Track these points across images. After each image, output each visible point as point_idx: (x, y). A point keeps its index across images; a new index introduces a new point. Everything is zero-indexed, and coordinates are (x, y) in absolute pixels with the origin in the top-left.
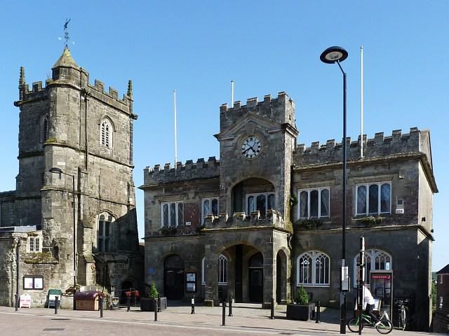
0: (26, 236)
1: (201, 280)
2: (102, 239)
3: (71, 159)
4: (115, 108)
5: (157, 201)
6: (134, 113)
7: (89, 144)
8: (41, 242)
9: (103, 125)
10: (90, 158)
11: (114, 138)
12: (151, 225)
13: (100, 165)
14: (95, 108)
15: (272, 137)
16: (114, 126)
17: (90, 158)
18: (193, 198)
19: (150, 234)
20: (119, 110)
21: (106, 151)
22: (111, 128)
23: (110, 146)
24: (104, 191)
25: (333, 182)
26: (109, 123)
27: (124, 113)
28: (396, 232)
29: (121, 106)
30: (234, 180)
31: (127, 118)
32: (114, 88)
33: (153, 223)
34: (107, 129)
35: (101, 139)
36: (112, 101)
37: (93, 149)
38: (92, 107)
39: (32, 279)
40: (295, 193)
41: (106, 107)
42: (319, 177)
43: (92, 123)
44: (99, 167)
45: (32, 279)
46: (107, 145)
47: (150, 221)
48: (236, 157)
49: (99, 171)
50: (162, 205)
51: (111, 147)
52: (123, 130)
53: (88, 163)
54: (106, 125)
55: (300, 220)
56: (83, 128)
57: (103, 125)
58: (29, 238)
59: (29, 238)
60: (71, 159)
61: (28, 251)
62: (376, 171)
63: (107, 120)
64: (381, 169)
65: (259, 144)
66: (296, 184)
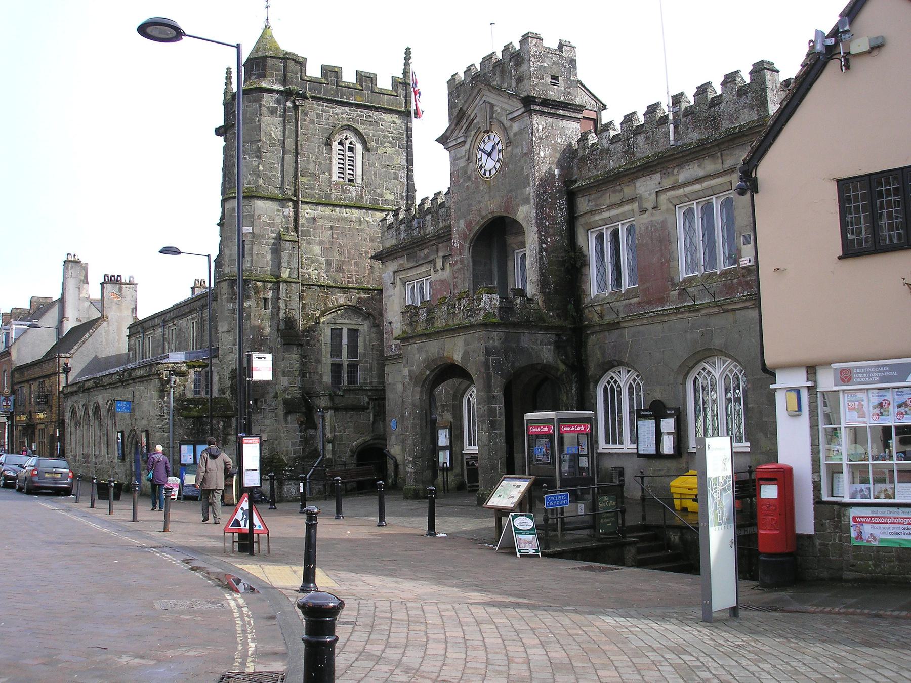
1: (462, 442)
3: (264, 218)
5: (398, 282)
8: (215, 378)
9: (341, 143)
10: (307, 212)
11: (366, 168)
13: (330, 219)
14: (319, 116)
15: (516, 127)
17: (307, 212)
18: (443, 269)
20: (377, 109)
21: (344, 191)
22: (359, 147)
23: (359, 180)
24: (339, 269)
25: (635, 206)
26: (353, 138)
27: (391, 111)
28: (743, 312)
29: (384, 102)
30: (469, 225)
32: (367, 69)
34: (351, 149)
38: (312, 115)
39: (191, 447)
40: (581, 241)
41: (347, 109)
42: (616, 198)
43: (311, 147)
44: (329, 224)
45: (191, 447)
48: (469, 178)
49: (330, 232)
50: (408, 288)
51: (359, 180)
53: (301, 221)
55: (596, 297)
56: (289, 158)
58: (192, 371)
60: (264, 218)
62: (701, 173)
63: (349, 134)
64: (710, 166)
65: (500, 147)
66: (582, 221)
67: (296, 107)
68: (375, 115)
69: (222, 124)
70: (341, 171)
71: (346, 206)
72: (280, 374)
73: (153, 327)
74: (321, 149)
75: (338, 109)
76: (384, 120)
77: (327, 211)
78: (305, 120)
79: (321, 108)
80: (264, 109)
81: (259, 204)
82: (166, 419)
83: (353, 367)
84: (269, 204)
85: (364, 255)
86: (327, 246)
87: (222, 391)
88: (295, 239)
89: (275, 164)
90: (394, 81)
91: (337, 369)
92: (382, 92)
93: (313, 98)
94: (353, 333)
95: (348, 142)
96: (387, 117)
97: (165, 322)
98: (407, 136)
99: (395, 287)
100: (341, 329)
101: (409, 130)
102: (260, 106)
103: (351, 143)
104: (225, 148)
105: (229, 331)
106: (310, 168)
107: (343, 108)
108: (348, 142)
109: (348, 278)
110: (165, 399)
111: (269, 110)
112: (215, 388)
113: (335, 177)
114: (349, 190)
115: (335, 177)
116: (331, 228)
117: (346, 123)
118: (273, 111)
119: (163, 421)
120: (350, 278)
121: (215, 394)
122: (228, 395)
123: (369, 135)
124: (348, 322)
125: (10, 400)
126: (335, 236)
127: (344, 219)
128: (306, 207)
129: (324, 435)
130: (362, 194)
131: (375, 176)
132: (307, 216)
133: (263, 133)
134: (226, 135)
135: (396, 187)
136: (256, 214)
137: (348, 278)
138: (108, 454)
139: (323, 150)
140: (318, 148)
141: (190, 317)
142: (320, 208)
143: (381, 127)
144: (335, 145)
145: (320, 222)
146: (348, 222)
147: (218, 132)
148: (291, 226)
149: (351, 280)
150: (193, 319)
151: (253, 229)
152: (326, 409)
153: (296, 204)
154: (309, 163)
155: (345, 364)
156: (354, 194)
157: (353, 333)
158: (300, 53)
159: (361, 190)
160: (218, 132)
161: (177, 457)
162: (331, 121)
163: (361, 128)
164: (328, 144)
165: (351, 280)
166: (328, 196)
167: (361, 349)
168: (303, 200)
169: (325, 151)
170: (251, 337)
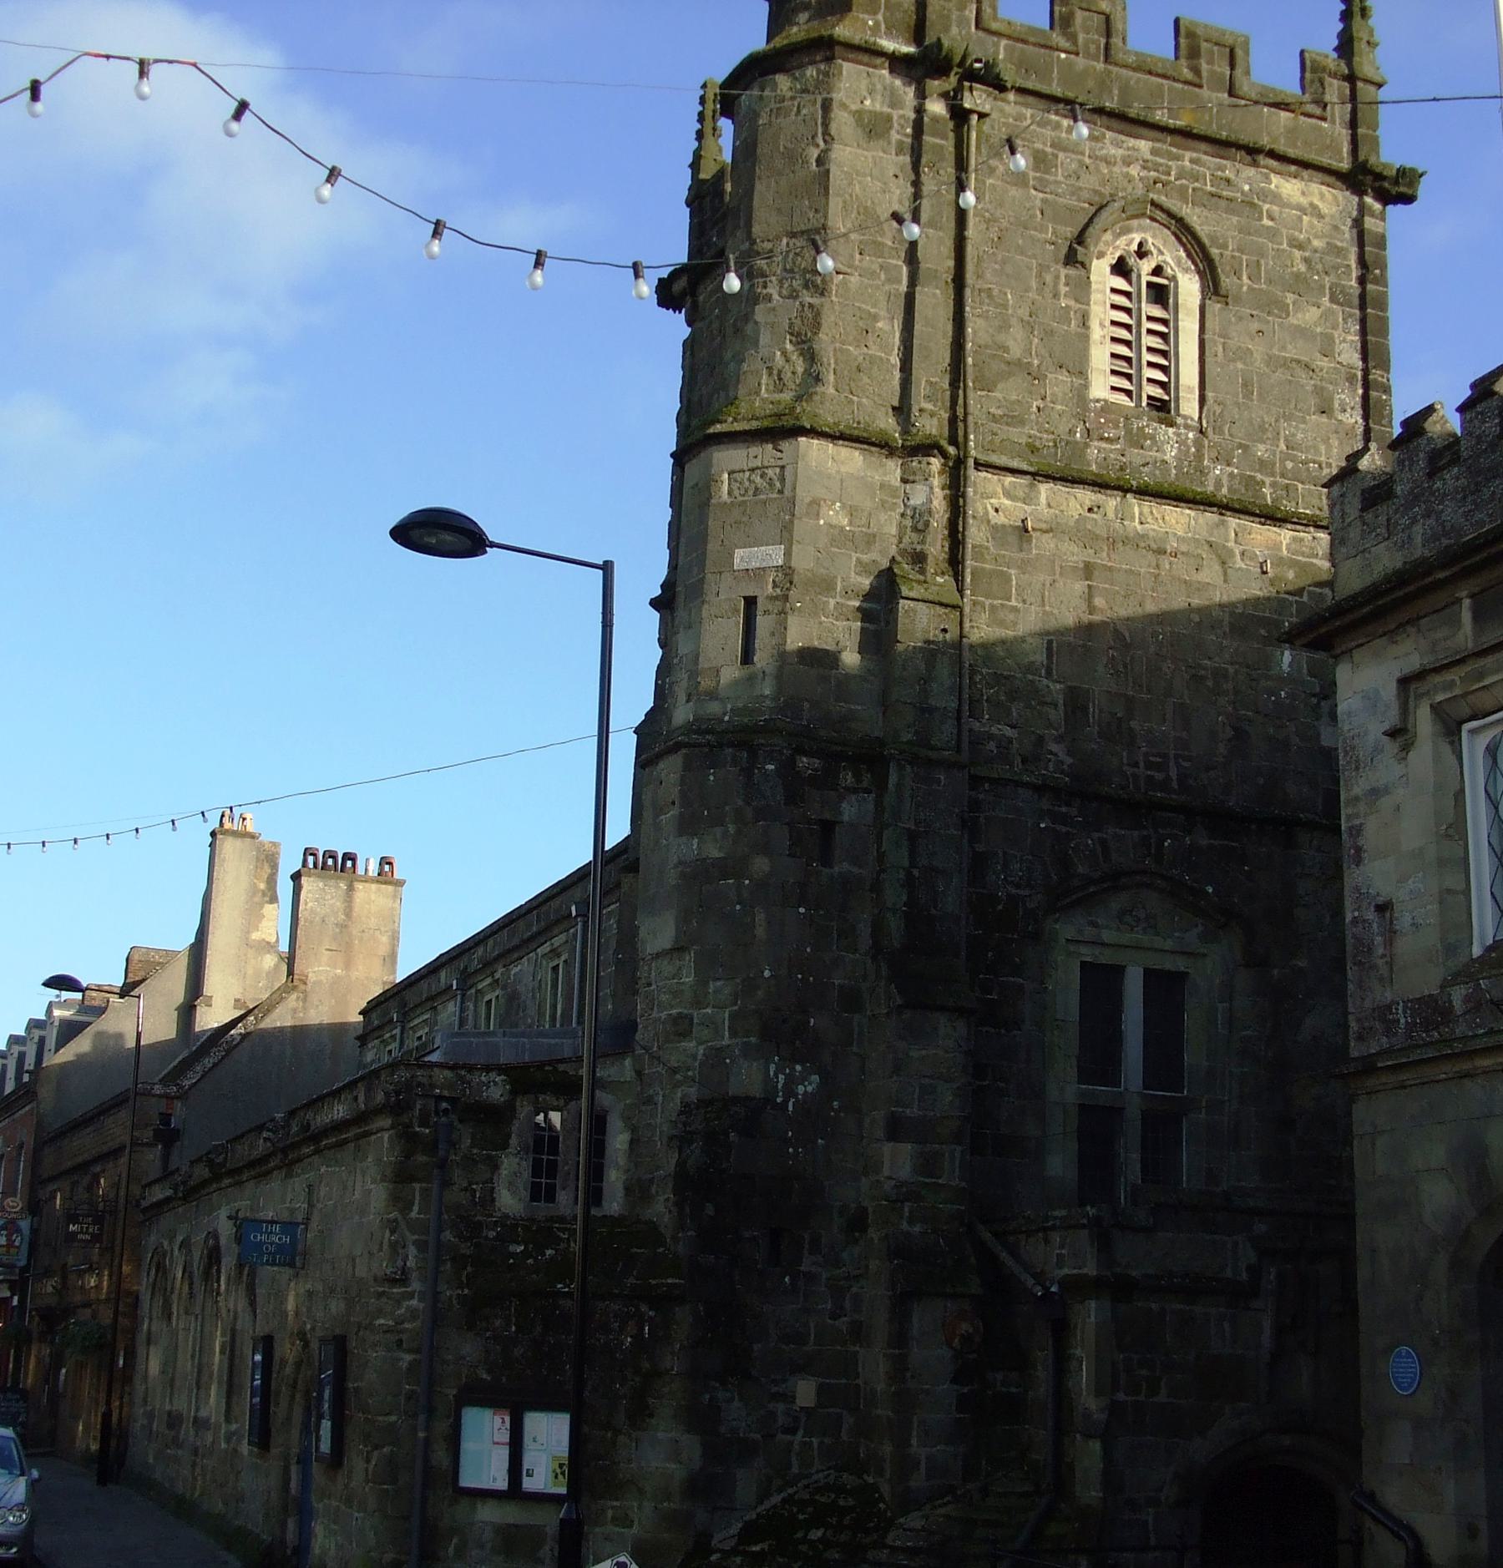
0: (496, 1090)
4: (1222, 145)
5: (1424, 722)
6: (1390, 154)
7: (977, 402)
8: (618, 1141)
9: (1121, 268)
11: (1216, 348)
12: (1391, 934)
13: (1083, 535)
14: (1040, 161)
19: (1390, 1026)
20: (1252, 152)
21: (1137, 440)
22: (1189, 288)
23: (1189, 406)
26: (1169, 254)
29: (1276, 128)
31: (1332, 201)
33: (1404, 921)
34: (1160, 294)
35: (1100, 356)
37: (1019, 435)
41: (1144, 146)
47: (1383, 908)
49: (1080, 586)
52: (1299, 285)
53: (975, 534)
56: (934, 302)
60: (835, 515)
61: (509, 1201)
67: (960, 116)
68: (1245, 177)
70: (1125, 366)
71: (1143, 492)
73: (432, 998)
74: (1049, 278)
75: (1115, 145)
76: (1276, 198)
78: (992, 170)
79: (1048, 133)
80: (842, 121)
81: (812, 449)
82: (411, 1296)
84: (851, 459)
85: (1210, 683)
87: (637, 1191)
88: (954, 598)
89: (875, 318)
93: (1022, 91)
95: (1146, 266)
96: (1290, 188)
97: (466, 979)
98: (1362, 262)
99: (1406, 748)
100: (1118, 971)
102: (827, 106)
103: (1158, 271)
104: (689, 346)
105: (678, 949)
106: (1011, 343)
107: (1132, 142)
108: (1146, 266)
109: (1149, 765)
110: (414, 1214)
112: (614, 1178)
113: (1101, 387)
114: (1152, 437)
115: (1101, 387)
116: (1088, 570)
118: (873, 128)
119: (398, 1303)
120: (1159, 767)
121: (614, 1204)
122: (661, 1209)
123: (1225, 246)
125: (19, 1231)
127: (1136, 542)
129: (1061, 1396)
130: (1199, 456)
131: (1248, 395)
132: (1000, 519)
133: (835, 204)
135: (1326, 441)
136: (803, 495)
137: (1149, 765)
138: (228, 1420)
139: (1056, 284)
140: (1039, 275)
141: (546, 948)
142: (1045, 489)
143: (1266, 222)
144: (1101, 271)
145: (1043, 545)
146: (1150, 556)
148: (936, 548)
149: (1159, 776)
150: (555, 953)
151: (788, 554)
152: (1076, 1287)
154: (1005, 326)
155: (1134, 1110)
156: (1171, 453)
159: (1196, 442)
161: (440, 1456)
162: (1089, 182)
163: (1194, 216)
165: (1159, 776)
166: (1079, 450)
168: (983, 458)
169: (1063, 289)
170: (767, 974)
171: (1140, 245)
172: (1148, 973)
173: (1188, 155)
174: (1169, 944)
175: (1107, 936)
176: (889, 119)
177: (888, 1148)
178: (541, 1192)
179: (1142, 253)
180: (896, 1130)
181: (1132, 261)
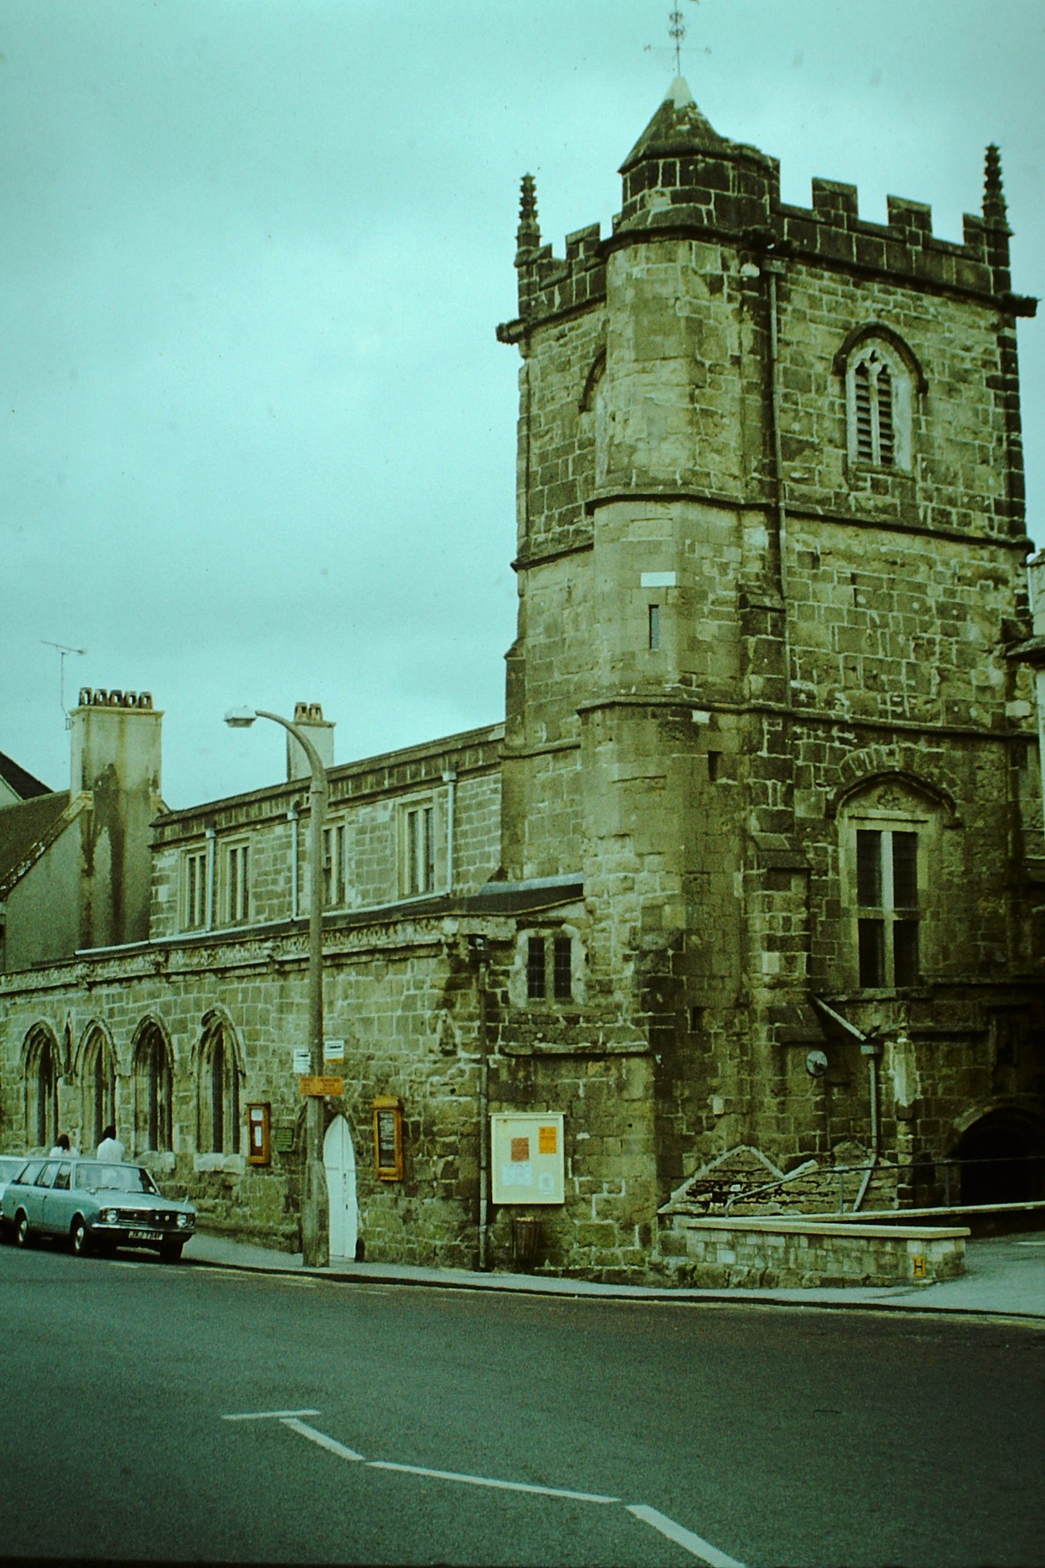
2: (880, 923)
6: (1019, 287)
9: (862, 371)
13: (849, 557)
16: (916, 366)
26: (890, 358)
36: (907, 254)
38: (799, 301)
44: (848, 570)
46: (887, 460)
53: (789, 561)
54: (875, 368)
57: (862, 371)
59: (523, 938)
69: (516, 315)
72: (758, 945)
77: (841, 537)
83: (906, 930)
86: (845, 624)
90: (968, 222)
91: (871, 929)
92: (943, 250)
94: (905, 843)
100: (878, 833)
101: (1008, 345)
109: (895, 704)
111: (705, 281)
116: (854, 579)
117: (873, 319)
124: (897, 814)
126: (861, 599)
128: (797, 525)
134: (528, 345)
145: (831, 565)
147: (505, 334)
149: (899, 710)
153: (773, 518)
157: (905, 843)
158: (768, 148)
160: (505, 334)
164: (840, 370)
165: (899, 710)
167: (922, 882)
171: (873, 353)
172: (896, 834)
173: (900, 291)
174: (907, 816)
175: (873, 813)
176: (721, 278)
177: (766, 955)
178: (536, 989)
179: (873, 359)
180: (771, 944)
181: (867, 364)
